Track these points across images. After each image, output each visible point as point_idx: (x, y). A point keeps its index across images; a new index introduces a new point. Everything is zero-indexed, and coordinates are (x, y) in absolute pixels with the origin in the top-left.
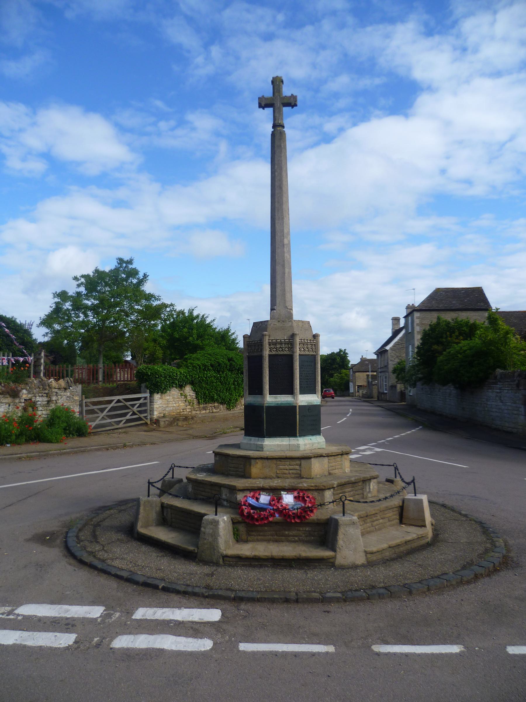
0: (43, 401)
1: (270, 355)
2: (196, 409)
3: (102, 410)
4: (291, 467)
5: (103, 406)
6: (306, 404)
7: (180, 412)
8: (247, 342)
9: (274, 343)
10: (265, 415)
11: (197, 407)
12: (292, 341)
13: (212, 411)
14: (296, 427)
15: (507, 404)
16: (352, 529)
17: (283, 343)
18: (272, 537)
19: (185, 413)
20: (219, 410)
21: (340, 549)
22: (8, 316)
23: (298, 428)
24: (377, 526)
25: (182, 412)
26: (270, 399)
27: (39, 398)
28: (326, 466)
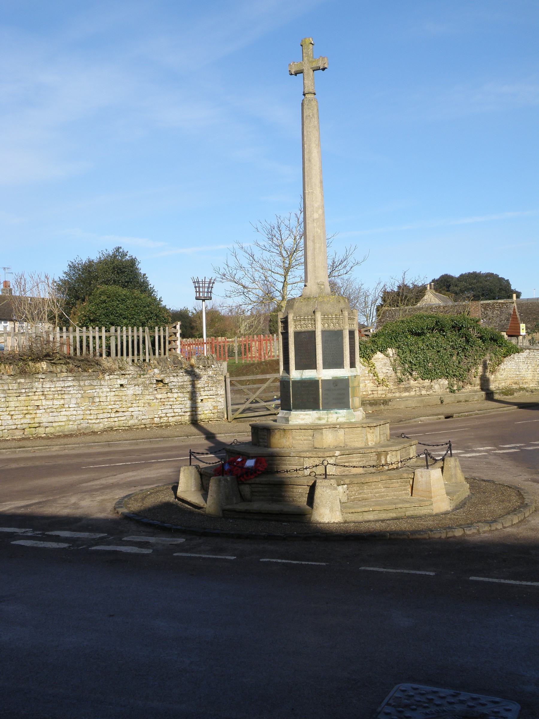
0: (178, 382)
1: (323, 332)
2: (394, 391)
3: (254, 391)
4: (305, 438)
5: (255, 386)
6: (331, 378)
7: (368, 395)
8: (281, 319)
9: (298, 320)
10: (291, 389)
11: (395, 388)
12: (314, 317)
13: (419, 394)
14: (319, 401)
15: (58, 369)
16: (330, 490)
17: (306, 319)
18: (271, 498)
19: (375, 396)
20: (432, 392)
21: (317, 507)
22: (163, 304)
23: (321, 401)
24: (378, 494)
25: (370, 394)
26: (295, 374)
27: (173, 378)
28: (342, 438)
